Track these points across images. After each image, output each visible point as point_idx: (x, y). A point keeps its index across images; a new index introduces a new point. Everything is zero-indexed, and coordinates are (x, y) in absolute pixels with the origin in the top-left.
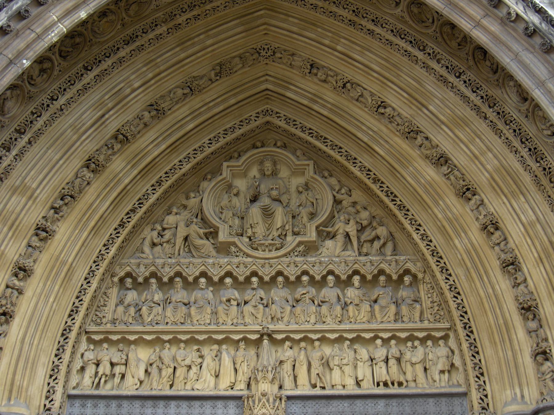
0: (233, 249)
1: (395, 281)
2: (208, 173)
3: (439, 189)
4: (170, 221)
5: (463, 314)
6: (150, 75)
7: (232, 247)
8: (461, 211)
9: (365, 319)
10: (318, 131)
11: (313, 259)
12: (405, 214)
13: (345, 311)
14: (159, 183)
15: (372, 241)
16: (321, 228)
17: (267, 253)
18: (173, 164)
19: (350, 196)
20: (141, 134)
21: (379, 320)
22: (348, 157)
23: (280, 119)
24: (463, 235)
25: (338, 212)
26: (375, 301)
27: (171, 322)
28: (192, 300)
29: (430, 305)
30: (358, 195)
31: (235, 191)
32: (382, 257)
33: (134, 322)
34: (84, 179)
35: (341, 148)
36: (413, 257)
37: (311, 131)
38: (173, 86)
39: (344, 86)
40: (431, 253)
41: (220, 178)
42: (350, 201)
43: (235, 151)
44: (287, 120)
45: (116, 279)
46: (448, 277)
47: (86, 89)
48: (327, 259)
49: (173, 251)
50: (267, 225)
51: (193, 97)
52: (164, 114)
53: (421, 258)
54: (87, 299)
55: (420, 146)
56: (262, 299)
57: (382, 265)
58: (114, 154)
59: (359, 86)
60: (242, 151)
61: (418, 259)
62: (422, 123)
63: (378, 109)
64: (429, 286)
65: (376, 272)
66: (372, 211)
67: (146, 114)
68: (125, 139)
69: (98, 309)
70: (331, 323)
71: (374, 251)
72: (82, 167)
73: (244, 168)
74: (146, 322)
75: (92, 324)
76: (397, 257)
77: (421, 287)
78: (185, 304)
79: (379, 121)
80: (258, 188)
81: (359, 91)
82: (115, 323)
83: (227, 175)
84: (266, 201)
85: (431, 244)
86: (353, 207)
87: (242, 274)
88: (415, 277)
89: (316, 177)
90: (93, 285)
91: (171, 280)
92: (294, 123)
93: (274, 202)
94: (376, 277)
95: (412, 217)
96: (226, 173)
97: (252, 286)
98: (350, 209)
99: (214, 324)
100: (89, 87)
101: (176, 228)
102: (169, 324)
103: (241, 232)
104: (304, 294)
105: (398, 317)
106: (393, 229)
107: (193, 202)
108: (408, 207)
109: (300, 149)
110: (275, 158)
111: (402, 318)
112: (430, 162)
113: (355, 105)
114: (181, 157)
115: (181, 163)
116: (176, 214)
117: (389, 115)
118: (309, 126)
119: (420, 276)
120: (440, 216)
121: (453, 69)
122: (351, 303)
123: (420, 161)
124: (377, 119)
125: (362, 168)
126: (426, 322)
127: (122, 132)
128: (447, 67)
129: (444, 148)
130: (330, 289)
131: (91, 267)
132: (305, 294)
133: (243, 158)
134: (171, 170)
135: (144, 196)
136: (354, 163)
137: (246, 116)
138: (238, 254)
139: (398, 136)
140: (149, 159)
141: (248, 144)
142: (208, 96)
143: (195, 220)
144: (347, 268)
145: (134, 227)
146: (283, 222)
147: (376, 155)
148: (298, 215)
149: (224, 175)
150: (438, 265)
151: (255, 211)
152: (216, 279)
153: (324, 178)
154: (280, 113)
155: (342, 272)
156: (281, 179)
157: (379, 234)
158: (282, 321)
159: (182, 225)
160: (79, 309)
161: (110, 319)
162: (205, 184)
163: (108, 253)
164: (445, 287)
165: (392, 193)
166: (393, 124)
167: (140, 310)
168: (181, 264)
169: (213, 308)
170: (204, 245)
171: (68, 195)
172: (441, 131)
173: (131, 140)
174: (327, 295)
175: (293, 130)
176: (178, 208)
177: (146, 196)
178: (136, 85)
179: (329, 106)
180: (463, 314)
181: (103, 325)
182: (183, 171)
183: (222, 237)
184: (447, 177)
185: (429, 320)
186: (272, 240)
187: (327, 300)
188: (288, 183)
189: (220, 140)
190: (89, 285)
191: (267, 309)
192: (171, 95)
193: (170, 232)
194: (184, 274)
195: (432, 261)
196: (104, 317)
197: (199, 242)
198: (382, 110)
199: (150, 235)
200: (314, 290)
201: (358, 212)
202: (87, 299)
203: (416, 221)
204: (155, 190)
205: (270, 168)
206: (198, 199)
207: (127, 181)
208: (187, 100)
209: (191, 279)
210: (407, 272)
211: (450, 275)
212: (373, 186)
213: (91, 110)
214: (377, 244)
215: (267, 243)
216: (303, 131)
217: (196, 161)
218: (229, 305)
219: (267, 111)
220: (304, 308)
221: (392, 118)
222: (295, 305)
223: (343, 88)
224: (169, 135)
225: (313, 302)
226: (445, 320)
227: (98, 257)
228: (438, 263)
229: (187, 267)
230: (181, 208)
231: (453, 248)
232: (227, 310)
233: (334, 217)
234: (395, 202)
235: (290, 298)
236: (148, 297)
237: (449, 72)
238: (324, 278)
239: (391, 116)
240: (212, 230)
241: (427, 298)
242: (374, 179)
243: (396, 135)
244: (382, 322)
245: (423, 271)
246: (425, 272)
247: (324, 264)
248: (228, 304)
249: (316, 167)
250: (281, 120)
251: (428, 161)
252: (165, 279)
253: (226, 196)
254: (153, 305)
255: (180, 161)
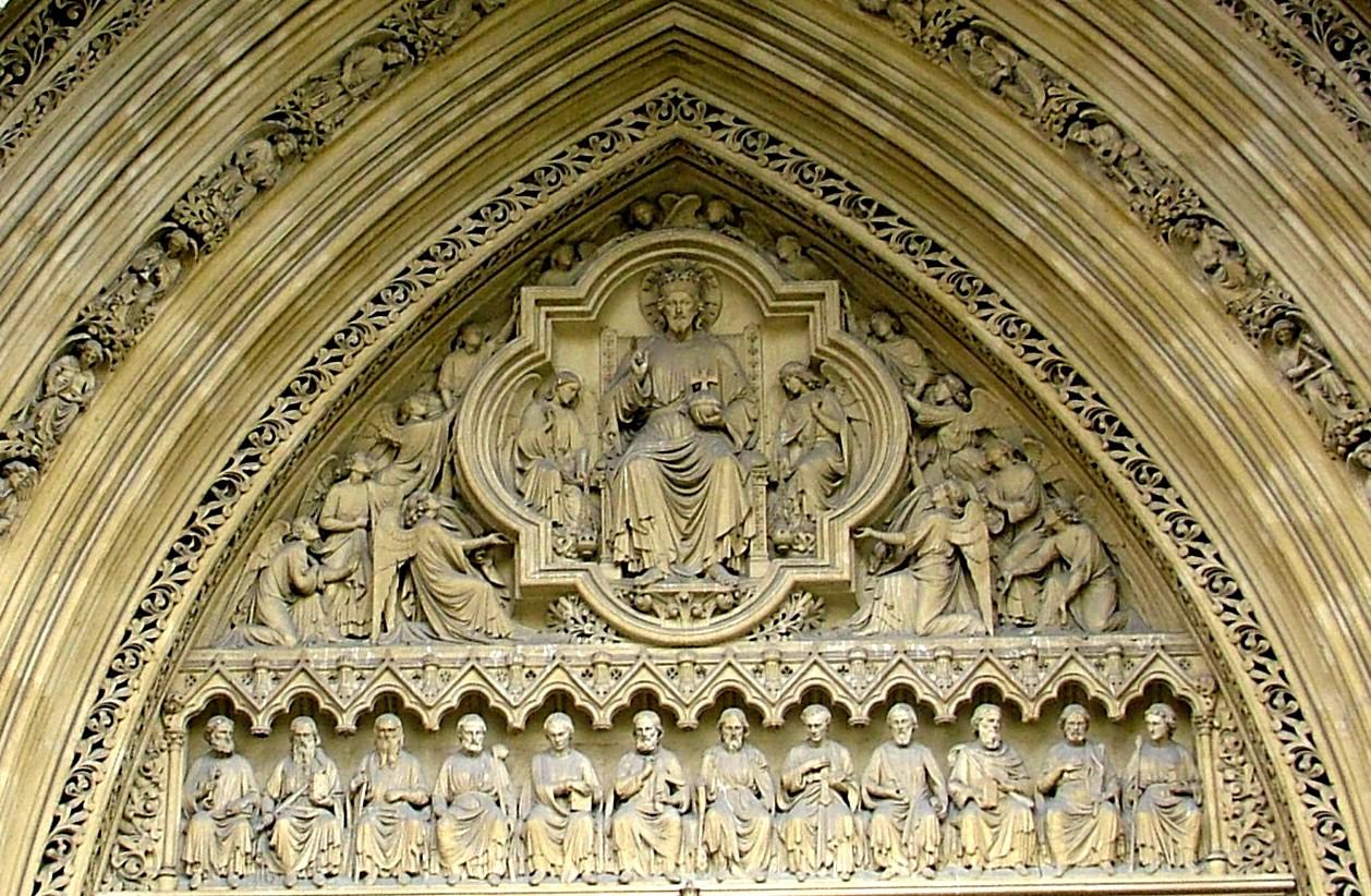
0: (569, 609)
1: (1117, 723)
2: (469, 322)
3: (1268, 420)
4: (344, 508)
5: (1335, 850)
6: (276, 17)
7: (563, 600)
8: (1338, 503)
9: (1014, 858)
10: (857, 181)
11: (843, 646)
12: (1156, 498)
13: (949, 829)
14: (311, 381)
15: (1040, 576)
16: (868, 531)
17: (686, 625)
18: (352, 311)
19: (967, 408)
20: (244, 219)
21: (1062, 860)
22: (961, 281)
23: (722, 133)
24: (1342, 587)
25: (923, 468)
26: (1050, 792)
27: (376, 871)
28: (440, 793)
29: (1233, 807)
30: (989, 407)
31: (566, 393)
32: (1076, 639)
33: (252, 870)
34: (68, 396)
35: (936, 248)
36: (1180, 640)
37: (831, 182)
38: (349, 42)
39: (950, 39)
40: (1238, 637)
41: (515, 346)
42: (966, 428)
43: (561, 242)
44: (748, 138)
45: (178, 722)
46: (1291, 721)
47: (62, 87)
48: (887, 647)
49: (362, 612)
50: (683, 523)
51: (420, 70)
52: (320, 142)
53: (1208, 649)
54: (96, 801)
55: (1211, 270)
56: (673, 788)
57: (1073, 668)
58: (157, 299)
59: (1001, 38)
60: (584, 239)
61: (1194, 646)
62: (1218, 187)
63: (1066, 127)
64: (1229, 740)
65: (1054, 694)
66: (1041, 468)
67: (262, 147)
68: (193, 242)
69: (128, 827)
70: (904, 871)
71: (1046, 616)
72: (58, 357)
73: (594, 307)
74: (292, 873)
75: (110, 879)
76: (1123, 639)
77: (1203, 744)
78: (417, 807)
79: (1072, 167)
80: (647, 382)
81: (1003, 63)
82: (190, 877)
83: (537, 338)
84: (677, 432)
85: (1238, 606)
86: (977, 447)
87: (604, 697)
88: (1183, 707)
89: (851, 343)
90: (113, 754)
91: (365, 719)
92: (772, 150)
93: (706, 435)
94: (1052, 709)
95: (1180, 509)
96: (534, 326)
97: (640, 744)
98: (966, 454)
99: (518, 875)
100: (74, 79)
101: (368, 528)
102: (370, 879)
103: (593, 543)
104: (814, 771)
105: (1124, 847)
106: (1113, 536)
107: (422, 433)
108: (1165, 470)
109: (792, 233)
110: (704, 265)
111: (1137, 851)
112: (1242, 328)
113: (987, 103)
114: (379, 286)
115: (380, 308)
116: (366, 478)
117: (1107, 153)
118: (825, 163)
119: (1201, 705)
120: (1269, 518)
121: (1326, 26)
122: (970, 799)
123: (1206, 315)
124: (1062, 160)
125: (1010, 323)
126: (1216, 865)
127: (183, 221)
128: (1306, 19)
129: (1289, 287)
130: (897, 749)
131: (101, 693)
132: (818, 770)
133: (595, 270)
134: (347, 332)
135: (260, 431)
136: (983, 305)
137: (598, 126)
138: (586, 628)
139: (1132, 224)
140: (275, 307)
141: (607, 215)
142: (467, 64)
143: (432, 503)
144: (957, 679)
145: (231, 543)
146: (738, 511)
147: (1058, 284)
148: (786, 480)
149: (528, 335)
150: (1259, 681)
151: (641, 472)
152: (517, 719)
153: (873, 343)
154: (721, 112)
155: (942, 688)
156: (721, 340)
157: (1065, 551)
158: (744, 866)
159: (387, 524)
160: (75, 839)
161: (169, 862)
162: (458, 366)
163: (152, 641)
164: (1281, 757)
165: (1110, 420)
166: (1119, 187)
167: (270, 827)
168: (395, 667)
169: (512, 820)
170: (467, 595)
171: (19, 458)
172: (1280, 226)
173: (212, 243)
174: (891, 776)
175: (768, 176)
176: (369, 453)
177: (268, 427)
178: (228, 58)
179: (898, 103)
180: (1335, 850)
181: (146, 881)
182: (390, 332)
183: (532, 566)
184: (1296, 386)
185: (1226, 860)
186: (701, 575)
187: (892, 792)
188: (749, 358)
189: (512, 215)
190: (99, 753)
191: (692, 824)
192: (346, 78)
193: (348, 544)
194: (409, 702)
195: (1239, 664)
196: (147, 853)
197: (450, 583)
198: (1083, 136)
199: (279, 558)
200: (845, 753)
201: (993, 469)
202: (96, 801)
203: (1189, 523)
204: (296, 407)
205: (685, 308)
206: (438, 426)
207: (205, 390)
208: (399, 84)
209: (431, 720)
210: (1158, 691)
211: (1298, 715)
212: (1047, 393)
213: (83, 157)
214: (1057, 588)
215: (683, 591)
216: (804, 182)
217: (431, 294)
218: (564, 811)
219: (676, 101)
220: (814, 821)
221: (1116, 163)
222: (782, 806)
223: (945, 44)
224: (343, 213)
225: (844, 795)
226: (1278, 858)
227: (122, 656)
228: (1260, 674)
229: (417, 677)
230: (380, 450)
231: (1309, 625)
232: (560, 828)
233: (912, 486)
234: (1119, 454)
235: (766, 787)
236: (292, 783)
237: (1310, 35)
238: (880, 711)
239: (1114, 156)
240: (492, 538)
241: (1220, 783)
242: (1049, 366)
243: (1127, 220)
244: (1073, 866)
245: (1211, 688)
246: (1217, 690)
247: (881, 666)
248: (560, 805)
249: (847, 302)
250: (723, 139)
251: (1236, 326)
252: (346, 722)
253: (535, 411)
254: (312, 812)
255: (377, 300)
